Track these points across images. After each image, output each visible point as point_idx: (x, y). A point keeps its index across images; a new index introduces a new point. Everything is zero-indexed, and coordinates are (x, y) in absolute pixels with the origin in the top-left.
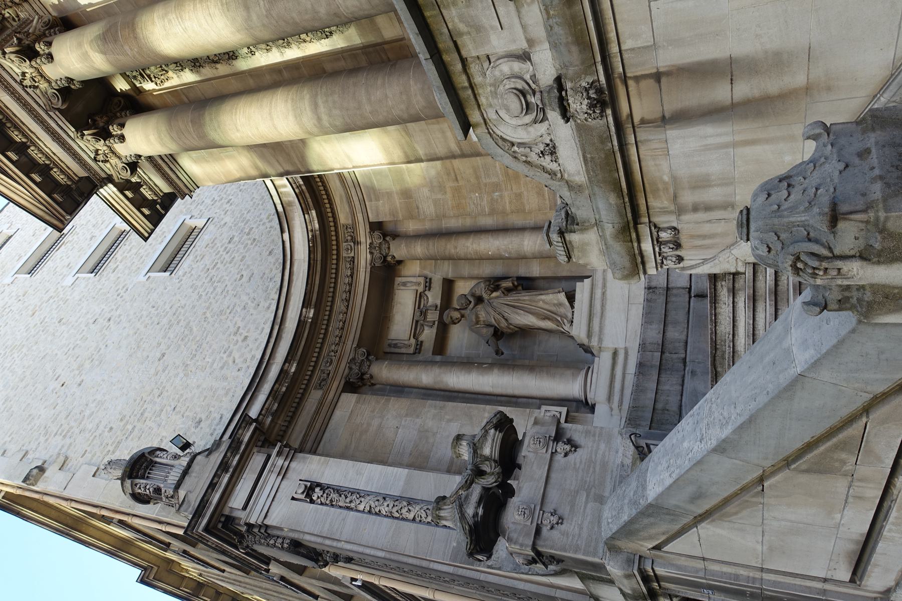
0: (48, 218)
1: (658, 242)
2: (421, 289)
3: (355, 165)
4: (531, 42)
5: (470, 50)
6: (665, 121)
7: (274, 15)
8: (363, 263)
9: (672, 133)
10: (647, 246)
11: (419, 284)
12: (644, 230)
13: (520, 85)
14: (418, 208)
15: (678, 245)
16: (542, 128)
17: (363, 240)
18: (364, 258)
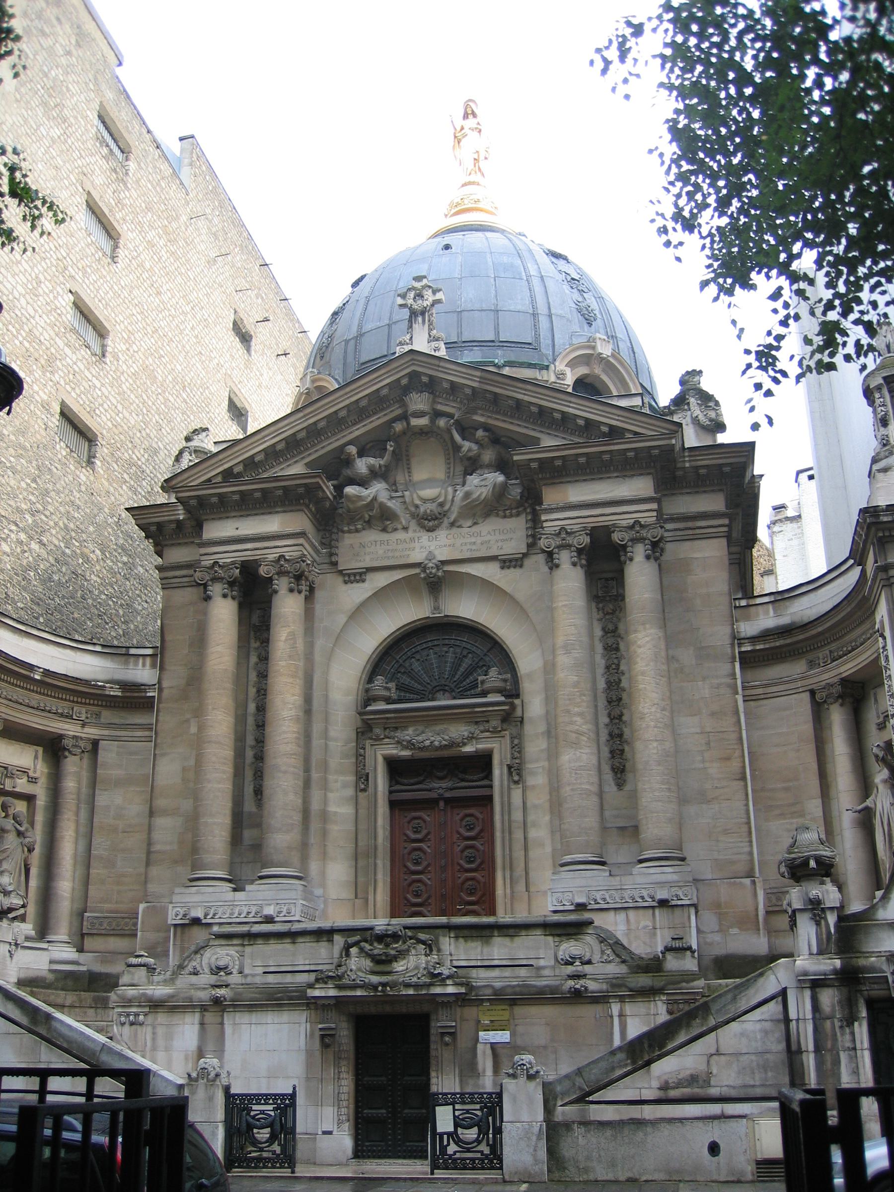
0: (179, 479)
1: (137, 1015)
2: (31, 774)
3: (158, 757)
4: (246, 976)
5: (248, 949)
6: (202, 1024)
8: (66, 726)
9: (196, 1027)
10: (134, 1010)
11: (35, 772)
12: (147, 1010)
13: (230, 967)
14: (105, 790)
15: (132, 1024)
16: (207, 970)
17: (86, 730)
18: (69, 729)
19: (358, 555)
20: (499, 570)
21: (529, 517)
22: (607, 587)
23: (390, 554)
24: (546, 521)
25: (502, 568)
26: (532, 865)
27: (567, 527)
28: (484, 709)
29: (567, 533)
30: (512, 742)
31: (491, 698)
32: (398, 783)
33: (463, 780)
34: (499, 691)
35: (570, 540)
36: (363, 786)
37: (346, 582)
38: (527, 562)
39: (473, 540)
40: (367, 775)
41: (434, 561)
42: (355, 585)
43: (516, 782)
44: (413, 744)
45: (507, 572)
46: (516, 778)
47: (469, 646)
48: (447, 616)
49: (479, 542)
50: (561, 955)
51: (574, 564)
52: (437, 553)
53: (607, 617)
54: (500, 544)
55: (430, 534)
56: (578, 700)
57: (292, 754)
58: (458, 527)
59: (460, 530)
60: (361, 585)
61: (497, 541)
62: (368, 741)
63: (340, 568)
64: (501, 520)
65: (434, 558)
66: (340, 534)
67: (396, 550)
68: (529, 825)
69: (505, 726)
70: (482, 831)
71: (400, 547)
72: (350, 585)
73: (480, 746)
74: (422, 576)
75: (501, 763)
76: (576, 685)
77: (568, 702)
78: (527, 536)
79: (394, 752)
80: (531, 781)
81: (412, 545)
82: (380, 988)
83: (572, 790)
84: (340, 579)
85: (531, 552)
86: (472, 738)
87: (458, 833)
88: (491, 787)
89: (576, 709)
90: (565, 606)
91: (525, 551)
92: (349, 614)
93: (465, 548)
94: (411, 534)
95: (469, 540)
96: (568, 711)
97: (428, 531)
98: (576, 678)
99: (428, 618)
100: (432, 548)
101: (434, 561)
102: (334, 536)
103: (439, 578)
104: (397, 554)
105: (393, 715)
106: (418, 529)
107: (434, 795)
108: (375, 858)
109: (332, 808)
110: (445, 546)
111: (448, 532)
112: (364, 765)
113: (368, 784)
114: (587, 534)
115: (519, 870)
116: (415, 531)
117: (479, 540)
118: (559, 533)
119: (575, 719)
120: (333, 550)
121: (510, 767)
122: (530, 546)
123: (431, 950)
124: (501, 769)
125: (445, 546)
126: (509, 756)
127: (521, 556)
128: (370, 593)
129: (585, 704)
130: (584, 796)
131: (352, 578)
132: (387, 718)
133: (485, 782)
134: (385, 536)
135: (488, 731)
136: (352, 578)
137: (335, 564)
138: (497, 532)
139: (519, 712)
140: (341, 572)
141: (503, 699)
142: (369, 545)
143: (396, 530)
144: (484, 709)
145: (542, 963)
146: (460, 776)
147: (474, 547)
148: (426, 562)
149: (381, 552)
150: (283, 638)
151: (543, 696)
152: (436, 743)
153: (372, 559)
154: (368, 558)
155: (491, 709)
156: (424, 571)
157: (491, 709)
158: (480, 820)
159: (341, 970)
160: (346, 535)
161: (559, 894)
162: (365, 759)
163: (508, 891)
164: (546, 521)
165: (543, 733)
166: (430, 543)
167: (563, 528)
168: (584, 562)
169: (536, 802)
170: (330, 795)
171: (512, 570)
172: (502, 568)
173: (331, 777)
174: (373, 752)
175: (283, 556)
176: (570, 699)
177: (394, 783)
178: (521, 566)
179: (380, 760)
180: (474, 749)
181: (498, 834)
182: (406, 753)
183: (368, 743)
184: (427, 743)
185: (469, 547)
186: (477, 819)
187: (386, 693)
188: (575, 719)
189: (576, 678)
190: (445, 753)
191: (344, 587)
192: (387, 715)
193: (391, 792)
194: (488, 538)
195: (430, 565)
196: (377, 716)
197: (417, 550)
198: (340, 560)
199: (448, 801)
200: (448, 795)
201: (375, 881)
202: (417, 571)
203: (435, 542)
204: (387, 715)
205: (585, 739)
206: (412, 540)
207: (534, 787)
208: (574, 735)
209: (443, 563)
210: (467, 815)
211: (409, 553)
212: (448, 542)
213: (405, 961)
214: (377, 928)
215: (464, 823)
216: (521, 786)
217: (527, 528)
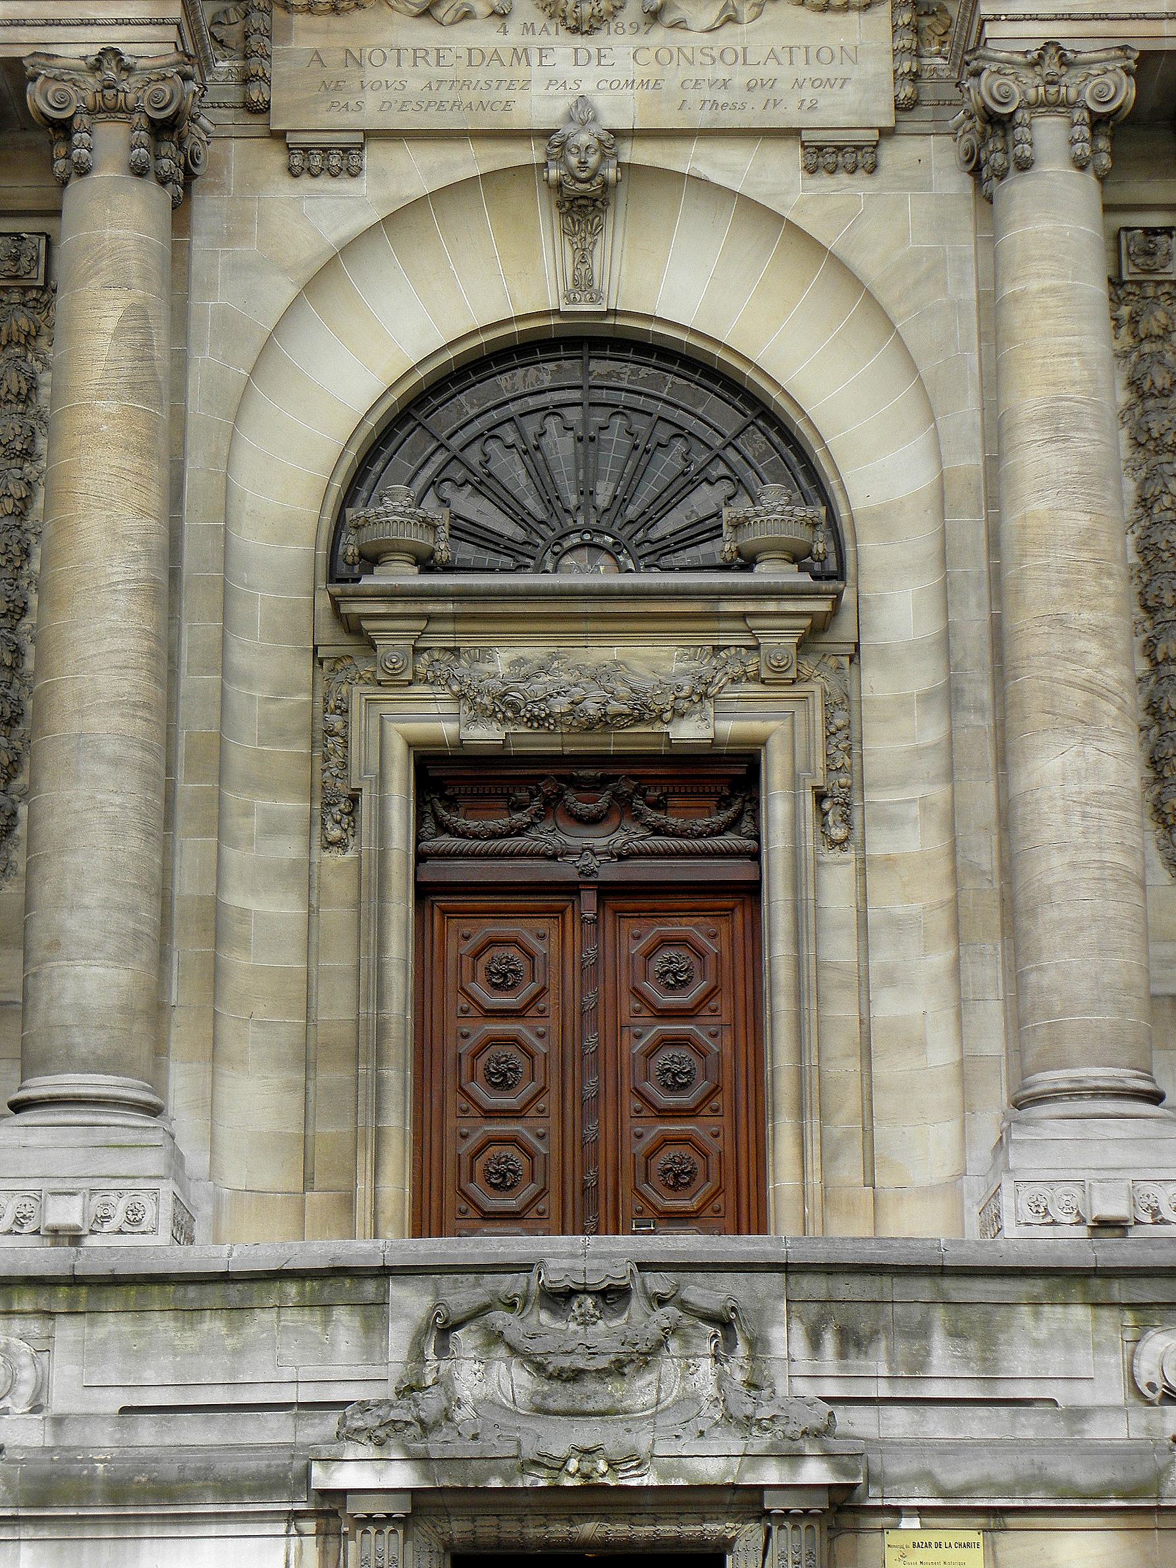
7: (90, 815)
19: (338, 88)
20: (801, 174)
21: (906, 17)
22: (1150, 254)
23: (447, 94)
24: (996, 18)
25: (811, 170)
26: (881, 1103)
27: (1064, 44)
28: (751, 607)
29: (1064, 62)
30: (828, 721)
31: (769, 573)
32: (443, 828)
33: (657, 831)
34: (798, 557)
35: (1072, 86)
36: (335, 833)
37: (293, 172)
38: (893, 155)
39: (722, 73)
40: (354, 799)
41: (594, 128)
42: (324, 183)
43: (840, 844)
44: (512, 705)
45: (824, 182)
46: (838, 833)
47: (676, 415)
48: (615, 313)
49: (739, 80)
50: (1146, 1371)
51: (1081, 165)
52: (601, 101)
53: (1147, 347)
54: (808, 93)
55: (579, 40)
56: (1091, 588)
57: (135, 705)
58: (674, 26)
59: (679, 35)
60: (345, 185)
61: (798, 84)
62: (356, 690)
63: (276, 127)
64: (816, 19)
65: (594, 119)
66: (278, 13)
67: (466, 84)
68: (874, 979)
69: (808, 666)
70: (711, 993)
71: (480, 75)
72: (306, 182)
73: (728, 728)
74: (554, 173)
75: (795, 780)
76: (1086, 539)
77: (1057, 591)
78: (897, 76)
79: (448, 729)
80: (880, 844)
81: (521, 71)
82: (573, 1465)
83: (1073, 865)
84: (276, 158)
85: (905, 127)
86: (704, 696)
87: (637, 993)
88: (755, 856)
89: (1086, 615)
90: (1053, 291)
91: (888, 122)
92: (305, 275)
93: (693, 96)
94: (514, 36)
95: (709, 73)
96: (1060, 621)
97: (575, 30)
98: (1084, 520)
99: (557, 312)
100: (587, 87)
101: (594, 128)
102: (256, 20)
103: (605, 185)
104: (471, 96)
105: (450, 608)
106: (539, 19)
107: (565, 871)
108: (380, 1060)
109: (236, 898)
110: (630, 84)
111: (639, 40)
112: (345, 766)
113: (354, 824)
114: (1128, 72)
115: (845, 1119)
116: (528, 28)
117: (740, 78)
118: (1037, 63)
119: (1081, 645)
120: (255, 66)
121: (820, 797)
122: (902, 107)
123: (730, 1346)
124: (795, 799)
125: (630, 84)
126: (820, 761)
127: (874, 135)
128: (375, 216)
129: (1110, 602)
130: (1111, 886)
131: (317, 161)
132: (429, 618)
133: (730, 840)
134: (425, 34)
135: (757, 679)
136: (317, 161)
137: (260, 110)
138: (800, 56)
139: (845, 629)
140: (279, 135)
141: (806, 578)
142: (377, 58)
143: (468, 15)
144: (751, 607)
145: (1084, 1395)
146: (653, 816)
147: (722, 97)
148: (569, 129)
149: (415, 85)
150: (110, 324)
151: (932, 580)
152: (591, 708)
153: (384, 106)
154: (371, 101)
155: (771, 607)
156: (561, 160)
157: (771, 607)
158: (710, 960)
159: (431, 1404)
160: (299, 20)
161: (1039, 1188)
162: (346, 746)
163: (814, 1179)
164: (996, 18)
165: (926, 698)
166: (577, 72)
167: (1051, 44)
168: (1105, 161)
169: (899, 909)
170: (232, 855)
171: (843, 177)
172: (811, 170)
173: (235, 798)
174: (374, 723)
175: (117, 53)
176: (1065, 584)
177: (429, 826)
178: (873, 169)
179: (398, 752)
180: (710, 734)
181: (782, 1004)
182: (486, 733)
183: (358, 694)
184: (560, 705)
185: (707, 94)
186: (700, 954)
187: (421, 538)
188: (1081, 645)
189: (1084, 520)
190: (611, 743)
191: (284, 190)
192: (432, 608)
193: (421, 857)
194: (770, 70)
195: (584, 139)
196: (399, 608)
197: (537, 89)
198: (277, 99)
199: (607, 891)
200: (611, 872)
201: (379, 1134)
202: (532, 154)
203: (593, 70)
204: (432, 608)
205: (1114, 711)
206: (520, 55)
207: (890, 862)
208: (1079, 696)
209: (617, 134)
210: (665, 942)
211: (504, 94)
212: (637, 72)
213: (650, 1377)
214: (552, 1263)
215: (656, 965)
216: (850, 855)
217: (896, 52)
